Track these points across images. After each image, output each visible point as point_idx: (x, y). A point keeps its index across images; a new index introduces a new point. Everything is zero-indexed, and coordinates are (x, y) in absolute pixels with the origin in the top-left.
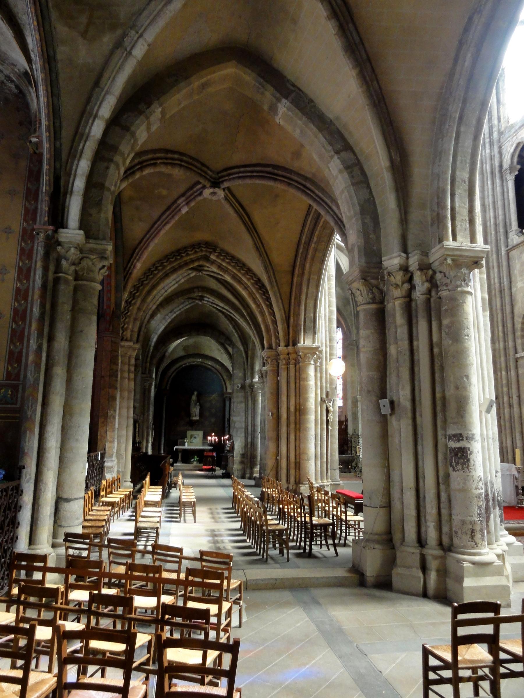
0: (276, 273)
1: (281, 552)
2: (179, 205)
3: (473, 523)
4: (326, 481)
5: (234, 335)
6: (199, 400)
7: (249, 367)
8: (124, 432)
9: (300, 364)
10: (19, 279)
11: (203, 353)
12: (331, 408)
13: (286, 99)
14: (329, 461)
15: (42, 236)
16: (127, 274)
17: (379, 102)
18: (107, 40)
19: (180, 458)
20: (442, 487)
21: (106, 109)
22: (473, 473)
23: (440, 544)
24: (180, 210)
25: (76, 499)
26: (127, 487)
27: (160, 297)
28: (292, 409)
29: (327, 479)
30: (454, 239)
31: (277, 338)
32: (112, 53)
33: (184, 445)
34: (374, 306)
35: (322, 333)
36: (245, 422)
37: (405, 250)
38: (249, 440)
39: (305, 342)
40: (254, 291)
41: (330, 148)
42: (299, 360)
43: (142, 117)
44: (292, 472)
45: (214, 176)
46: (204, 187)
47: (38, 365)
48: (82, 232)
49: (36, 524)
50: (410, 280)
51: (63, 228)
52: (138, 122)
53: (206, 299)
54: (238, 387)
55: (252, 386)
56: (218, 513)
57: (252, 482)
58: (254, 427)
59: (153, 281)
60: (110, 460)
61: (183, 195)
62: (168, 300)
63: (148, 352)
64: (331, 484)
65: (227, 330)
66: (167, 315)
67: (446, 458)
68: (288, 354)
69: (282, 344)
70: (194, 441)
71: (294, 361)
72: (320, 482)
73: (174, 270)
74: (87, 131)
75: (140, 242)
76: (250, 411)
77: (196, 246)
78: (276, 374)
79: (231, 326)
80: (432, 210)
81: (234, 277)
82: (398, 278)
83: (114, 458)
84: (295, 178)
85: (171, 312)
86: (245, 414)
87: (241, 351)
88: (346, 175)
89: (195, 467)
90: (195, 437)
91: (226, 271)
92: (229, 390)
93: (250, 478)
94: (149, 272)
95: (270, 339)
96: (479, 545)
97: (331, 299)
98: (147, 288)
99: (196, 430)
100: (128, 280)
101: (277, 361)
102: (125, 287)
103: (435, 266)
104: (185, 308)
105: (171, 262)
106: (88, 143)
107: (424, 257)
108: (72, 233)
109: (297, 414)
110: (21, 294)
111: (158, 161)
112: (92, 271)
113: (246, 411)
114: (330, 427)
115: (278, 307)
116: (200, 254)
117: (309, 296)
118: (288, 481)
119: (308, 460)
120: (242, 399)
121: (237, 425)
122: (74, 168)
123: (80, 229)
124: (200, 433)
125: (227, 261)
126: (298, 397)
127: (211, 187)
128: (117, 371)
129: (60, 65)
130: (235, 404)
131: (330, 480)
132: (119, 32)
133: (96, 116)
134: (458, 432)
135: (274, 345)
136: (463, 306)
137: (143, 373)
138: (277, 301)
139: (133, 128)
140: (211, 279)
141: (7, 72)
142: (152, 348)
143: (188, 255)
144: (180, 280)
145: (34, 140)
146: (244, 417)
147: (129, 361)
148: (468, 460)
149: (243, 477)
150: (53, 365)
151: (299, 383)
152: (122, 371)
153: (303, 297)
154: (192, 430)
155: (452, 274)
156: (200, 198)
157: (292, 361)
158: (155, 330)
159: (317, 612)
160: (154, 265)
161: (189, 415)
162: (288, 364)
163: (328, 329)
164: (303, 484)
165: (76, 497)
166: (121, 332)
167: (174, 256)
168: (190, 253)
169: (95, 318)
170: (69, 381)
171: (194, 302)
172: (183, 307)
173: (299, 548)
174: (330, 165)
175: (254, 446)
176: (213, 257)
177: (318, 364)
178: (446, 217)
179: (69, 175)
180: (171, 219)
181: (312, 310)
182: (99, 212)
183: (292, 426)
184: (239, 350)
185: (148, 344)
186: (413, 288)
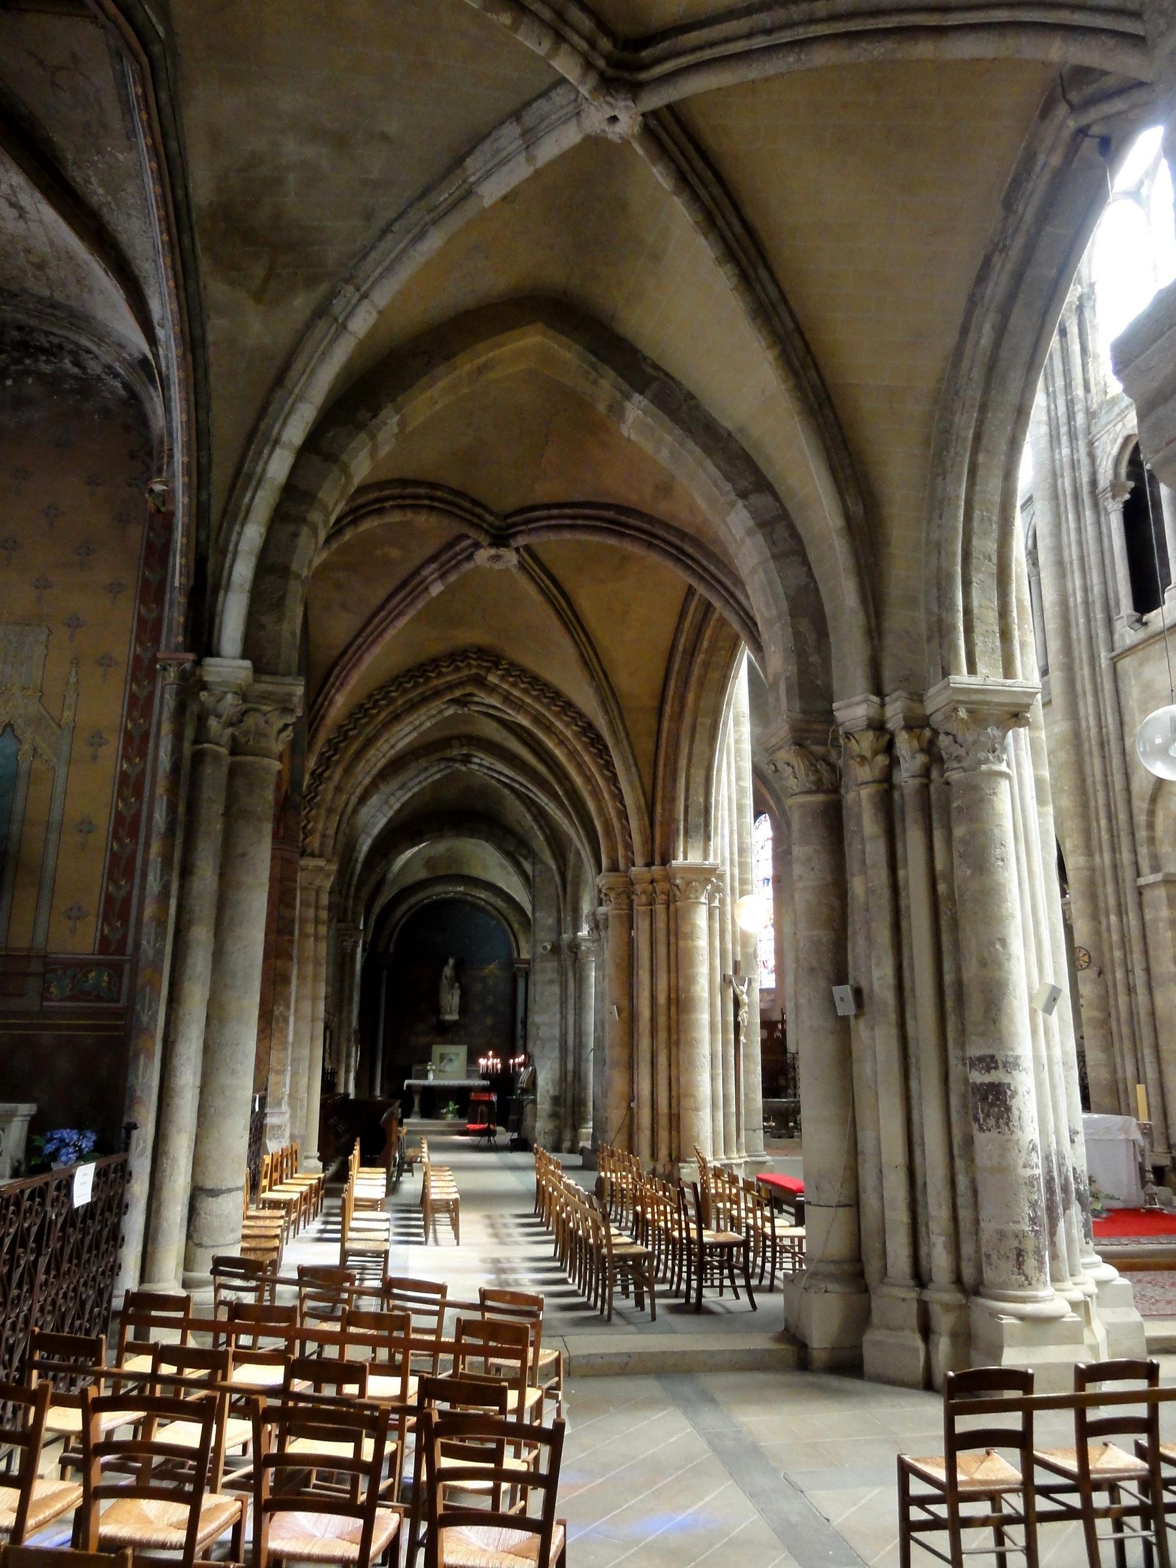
0: (626, 715)
1: (640, 1303)
2: (425, 578)
3: (1019, 1236)
4: (735, 1155)
5: (537, 837)
6: (458, 976)
7: (569, 907)
8: (306, 1052)
9: (678, 903)
10: (126, 756)
11: (466, 872)
12: (745, 996)
13: (642, 393)
14: (743, 1110)
15: (172, 674)
16: (316, 716)
17: (820, 406)
18: (302, 303)
19: (416, 1109)
20: (959, 1164)
21: (295, 431)
22: (1018, 1134)
23: (958, 1281)
24: (426, 589)
25: (230, 1190)
26: (311, 1171)
27: (379, 760)
28: (662, 998)
29: (738, 1150)
30: (972, 670)
31: (629, 847)
32: (309, 325)
33: (426, 1078)
34: (820, 798)
35: (723, 836)
37: (878, 690)
38: (570, 1066)
39: (687, 857)
40: (579, 748)
41: (728, 487)
42: (675, 896)
43: (363, 435)
44: (663, 1134)
45: (497, 523)
46: (477, 545)
47: (161, 923)
48: (247, 663)
49: (155, 1239)
50: (889, 748)
51: (212, 655)
52: (354, 444)
54: (545, 948)
55: (574, 946)
56: (505, 1226)
57: (577, 1160)
58: (580, 1037)
59: (369, 729)
60: (277, 1110)
61: (433, 559)
62: (396, 766)
64: (746, 1162)
65: (519, 823)
66: (393, 794)
67: (965, 1106)
68: (652, 882)
69: (639, 860)
70: (448, 1069)
71: (664, 897)
72: (723, 1157)
73: (412, 707)
74: (259, 469)
75: (344, 653)
76: (571, 1002)
77: (457, 656)
78: (627, 924)
79: (529, 817)
80: (929, 612)
81: (537, 719)
82: (865, 743)
83: (285, 1107)
84: (661, 533)
85: (401, 788)
86: (561, 1006)
87: (551, 869)
88: (760, 538)
89: (450, 1125)
90: (451, 1060)
91: (520, 707)
92: (525, 955)
93: (572, 1150)
94: (360, 712)
95: (613, 849)
96: (1033, 1282)
97: (742, 764)
98: (355, 746)
99: (452, 1043)
100: (316, 730)
101: (629, 897)
102: (310, 745)
103: (937, 719)
104: (430, 780)
105: (406, 691)
106: (260, 493)
107: (916, 705)
108: (229, 666)
109: (673, 1009)
110: (130, 785)
111: (387, 504)
112: (266, 736)
113: (563, 1003)
114: (742, 1038)
115: (631, 783)
116: (466, 672)
117: (694, 760)
118: (654, 1155)
119: (697, 1110)
120: (555, 976)
121: (544, 1032)
122: (234, 538)
123: (244, 656)
124: (461, 1051)
125: (522, 686)
126: (673, 975)
127: (491, 545)
128: (293, 921)
129: (211, 350)
130: (538, 986)
131: (744, 1154)
132: (324, 288)
133: (277, 442)
134: (988, 1052)
135: (622, 863)
136: (991, 801)
137: (339, 921)
138: (628, 770)
139: (345, 457)
140: (489, 720)
141: (107, 359)
142: (359, 866)
143: (440, 675)
144: (421, 725)
145: (158, 488)
147: (317, 901)
148: (1008, 1109)
149: (557, 1149)
150: (190, 924)
151: (677, 944)
152: (303, 921)
153: (683, 763)
154: (444, 1043)
155: (970, 738)
156: (468, 566)
157: (661, 898)
159: (709, 1418)
160: (370, 696)
161: (437, 1009)
162: (651, 903)
163: (735, 828)
164: (686, 1162)
165: (230, 1186)
166: (302, 836)
167: (413, 676)
168: (444, 670)
169: (268, 828)
170: (219, 955)
171: (449, 767)
172: (426, 778)
173: (677, 1294)
174: (728, 519)
175: (579, 1079)
176: (493, 679)
177: (716, 903)
178: (954, 627)
179: (224, 553)
180: (407, 606)
181: (701, 791)
182: (280, 620)
183: (662, 1035)
185: (351, 859)
186: (894, 762)
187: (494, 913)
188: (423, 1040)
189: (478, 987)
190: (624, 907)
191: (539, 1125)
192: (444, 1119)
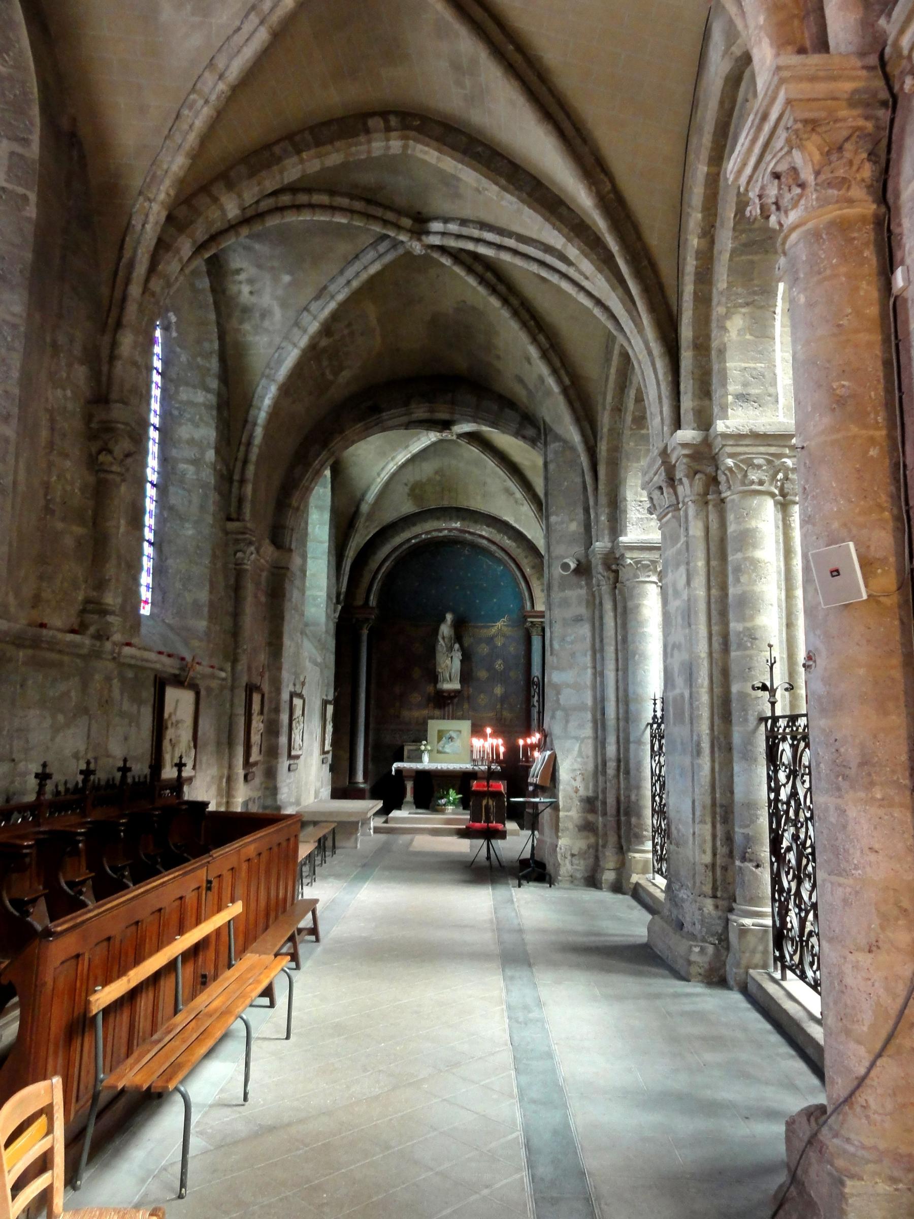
7: (603, 500)
11: (464, 504)
19: (409, 797)
33: (419, 759)
36: (594, 688)
38: (611, 750)
53: (436, 226)
54: (565, 566)
55: (613, 562)
58: (627, 704)
63: (249, 444)
65: (520, 380)
66: (306, 309)
76: (610, 650)
78: (869, 254)
85: (317, 298)
87: (573, 449)
89: (449, 821)
90: (451, 738)
92: (540, 607)
93: (617, 888)
99: (454, 717)
104: (364, 276)
113: (597, 651)
120: (583, 610)
121: (568, 697)
130: (558, 629)
142: (259, 432)
146: (589, 671)
149: (592, 881)
154: (443, 718)
158: (268, 366)
161: (433, 677)
175: (627, 772)
184: (567, 445)
187: (500, 554)
188: (417, 714)
189: (484, 649)
190: (858, 192)
191: (563, 842)
192: (442, 812)
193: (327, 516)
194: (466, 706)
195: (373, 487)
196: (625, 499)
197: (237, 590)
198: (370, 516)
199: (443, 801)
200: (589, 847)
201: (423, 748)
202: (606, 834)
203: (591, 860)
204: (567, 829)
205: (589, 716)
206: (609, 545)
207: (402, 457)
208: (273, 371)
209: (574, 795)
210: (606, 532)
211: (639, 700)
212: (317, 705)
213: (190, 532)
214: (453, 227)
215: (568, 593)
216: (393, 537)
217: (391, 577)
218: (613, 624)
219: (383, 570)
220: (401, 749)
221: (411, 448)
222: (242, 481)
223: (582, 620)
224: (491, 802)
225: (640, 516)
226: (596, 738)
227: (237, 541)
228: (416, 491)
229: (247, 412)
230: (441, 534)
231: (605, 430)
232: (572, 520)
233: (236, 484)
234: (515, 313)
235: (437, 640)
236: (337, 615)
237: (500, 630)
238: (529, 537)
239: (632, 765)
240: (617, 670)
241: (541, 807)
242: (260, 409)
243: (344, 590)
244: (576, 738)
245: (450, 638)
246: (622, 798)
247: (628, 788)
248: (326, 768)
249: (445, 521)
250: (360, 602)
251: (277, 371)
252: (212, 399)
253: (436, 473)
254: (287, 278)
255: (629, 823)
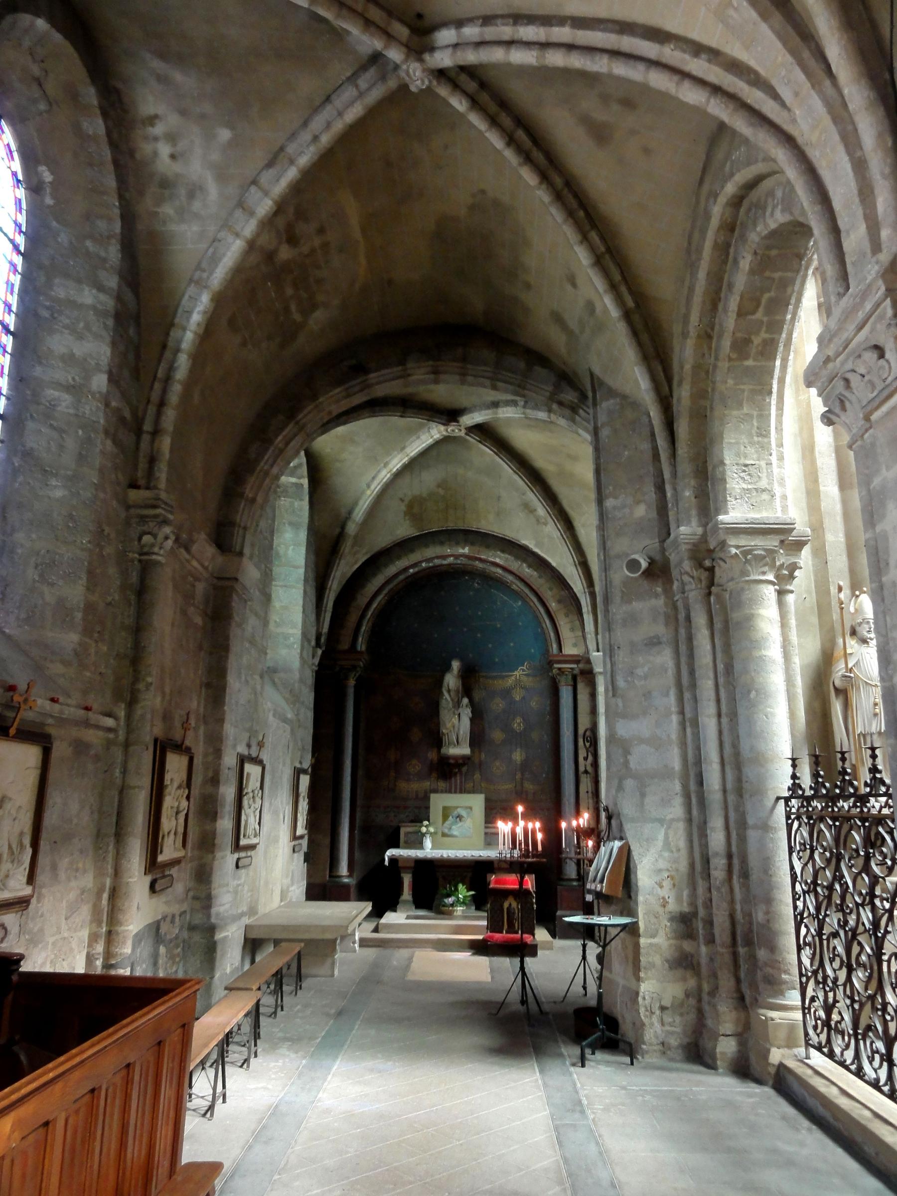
6: (467, 690)
7: (685, 467)
19: (407, 895)
33: (420, 845)
36: (683, 744)
38: (717, 839)
54: (633, 565)
55: (707, 557)
58: (738, 767)
63: (168, 379)
65: (558, 319)
66: (254, 182)
70: (458, 830)
76: (707, 686)
85: (270, 164)
87: (635, 405)
89: (459, 930)
90: (460, 817)
92: (569, 650)
93: (743, 1069)
104: (339, 126)
113: (686, 686)
120: (661, 629)
121: (642, 758)
124: (477, 802)
142: (183, 362)
146: (675, 719)
149: (697, 1053)
158: (198, 267)
161: (437, 740)
175: (745, 875)
184: (628, 402)
185: (164, 347)
187: (517, 586)
188: (416, 786)
189: (498, 705)
191: (648, 988)
193: (303, 535)
194: (477, 776)
195: (361, 503)
196: (722, 463)
197: (141, 594)
198: (358, 540)
199: (450, 900)
200: (687, 995)
201: (424, 830)
202: (714, 975)
203: (692, 1016)
204: (652, 965)
205: (677, 786)
206: (700, 531)
207: (397, 462)
208: (205, 275)
209: (661, 910)
210: (694, 512)
211: (761, 760)
212: (287, 775)
213: (59, 493)
214: (471, 32)
215: (637, 605)
216: (386, 565)
217: (384, 615)
218: (709, 647)
219: (374, 605)
220: (397, 831)
221: (408, 450)
222: (156, 432)
223: (660, 643)
224: (514, 904)
225: (745, 486)
226: (689, 820)
227: (143, 519)
228: (415, 509)
229: (168, 334)
230: (445, 562)
231: (688, 367)
232: (638, 503)
233: (146, 438)
234: (558, 197)
235: (441, 694)
236: (317, 661)
237: (518, 682)
238: (554, 564)
239: (754, 862)
240: (719, 715)
241: (613, 932)
242: (184, 329)
243: (325, 629)
244: (661, 821)
245: (457, 691)
246: (739, 916)
247: (749, 899)
248: (300, 858)
249: (450, 547)
250: (345, 646)
251: (211, 273)
252: (109, 303)
253: (439, 486)
254: (225, 134)
255: (753, 958)
